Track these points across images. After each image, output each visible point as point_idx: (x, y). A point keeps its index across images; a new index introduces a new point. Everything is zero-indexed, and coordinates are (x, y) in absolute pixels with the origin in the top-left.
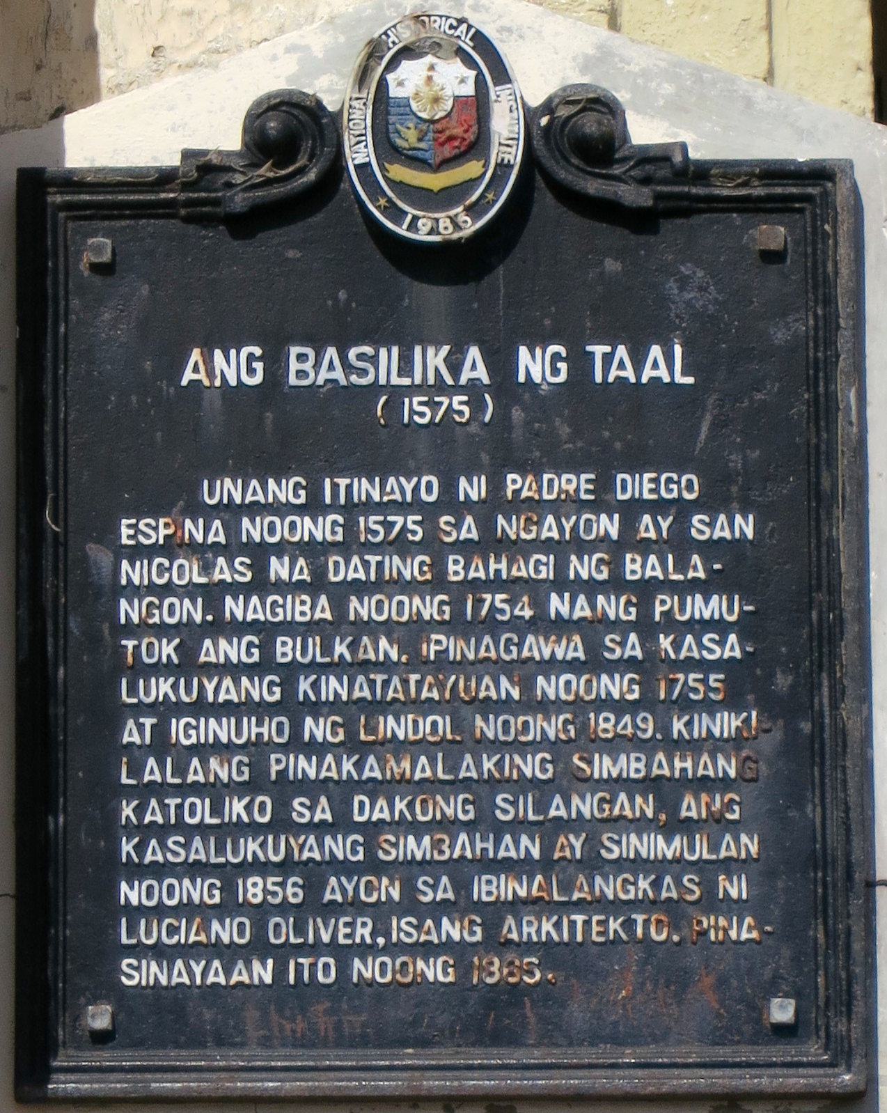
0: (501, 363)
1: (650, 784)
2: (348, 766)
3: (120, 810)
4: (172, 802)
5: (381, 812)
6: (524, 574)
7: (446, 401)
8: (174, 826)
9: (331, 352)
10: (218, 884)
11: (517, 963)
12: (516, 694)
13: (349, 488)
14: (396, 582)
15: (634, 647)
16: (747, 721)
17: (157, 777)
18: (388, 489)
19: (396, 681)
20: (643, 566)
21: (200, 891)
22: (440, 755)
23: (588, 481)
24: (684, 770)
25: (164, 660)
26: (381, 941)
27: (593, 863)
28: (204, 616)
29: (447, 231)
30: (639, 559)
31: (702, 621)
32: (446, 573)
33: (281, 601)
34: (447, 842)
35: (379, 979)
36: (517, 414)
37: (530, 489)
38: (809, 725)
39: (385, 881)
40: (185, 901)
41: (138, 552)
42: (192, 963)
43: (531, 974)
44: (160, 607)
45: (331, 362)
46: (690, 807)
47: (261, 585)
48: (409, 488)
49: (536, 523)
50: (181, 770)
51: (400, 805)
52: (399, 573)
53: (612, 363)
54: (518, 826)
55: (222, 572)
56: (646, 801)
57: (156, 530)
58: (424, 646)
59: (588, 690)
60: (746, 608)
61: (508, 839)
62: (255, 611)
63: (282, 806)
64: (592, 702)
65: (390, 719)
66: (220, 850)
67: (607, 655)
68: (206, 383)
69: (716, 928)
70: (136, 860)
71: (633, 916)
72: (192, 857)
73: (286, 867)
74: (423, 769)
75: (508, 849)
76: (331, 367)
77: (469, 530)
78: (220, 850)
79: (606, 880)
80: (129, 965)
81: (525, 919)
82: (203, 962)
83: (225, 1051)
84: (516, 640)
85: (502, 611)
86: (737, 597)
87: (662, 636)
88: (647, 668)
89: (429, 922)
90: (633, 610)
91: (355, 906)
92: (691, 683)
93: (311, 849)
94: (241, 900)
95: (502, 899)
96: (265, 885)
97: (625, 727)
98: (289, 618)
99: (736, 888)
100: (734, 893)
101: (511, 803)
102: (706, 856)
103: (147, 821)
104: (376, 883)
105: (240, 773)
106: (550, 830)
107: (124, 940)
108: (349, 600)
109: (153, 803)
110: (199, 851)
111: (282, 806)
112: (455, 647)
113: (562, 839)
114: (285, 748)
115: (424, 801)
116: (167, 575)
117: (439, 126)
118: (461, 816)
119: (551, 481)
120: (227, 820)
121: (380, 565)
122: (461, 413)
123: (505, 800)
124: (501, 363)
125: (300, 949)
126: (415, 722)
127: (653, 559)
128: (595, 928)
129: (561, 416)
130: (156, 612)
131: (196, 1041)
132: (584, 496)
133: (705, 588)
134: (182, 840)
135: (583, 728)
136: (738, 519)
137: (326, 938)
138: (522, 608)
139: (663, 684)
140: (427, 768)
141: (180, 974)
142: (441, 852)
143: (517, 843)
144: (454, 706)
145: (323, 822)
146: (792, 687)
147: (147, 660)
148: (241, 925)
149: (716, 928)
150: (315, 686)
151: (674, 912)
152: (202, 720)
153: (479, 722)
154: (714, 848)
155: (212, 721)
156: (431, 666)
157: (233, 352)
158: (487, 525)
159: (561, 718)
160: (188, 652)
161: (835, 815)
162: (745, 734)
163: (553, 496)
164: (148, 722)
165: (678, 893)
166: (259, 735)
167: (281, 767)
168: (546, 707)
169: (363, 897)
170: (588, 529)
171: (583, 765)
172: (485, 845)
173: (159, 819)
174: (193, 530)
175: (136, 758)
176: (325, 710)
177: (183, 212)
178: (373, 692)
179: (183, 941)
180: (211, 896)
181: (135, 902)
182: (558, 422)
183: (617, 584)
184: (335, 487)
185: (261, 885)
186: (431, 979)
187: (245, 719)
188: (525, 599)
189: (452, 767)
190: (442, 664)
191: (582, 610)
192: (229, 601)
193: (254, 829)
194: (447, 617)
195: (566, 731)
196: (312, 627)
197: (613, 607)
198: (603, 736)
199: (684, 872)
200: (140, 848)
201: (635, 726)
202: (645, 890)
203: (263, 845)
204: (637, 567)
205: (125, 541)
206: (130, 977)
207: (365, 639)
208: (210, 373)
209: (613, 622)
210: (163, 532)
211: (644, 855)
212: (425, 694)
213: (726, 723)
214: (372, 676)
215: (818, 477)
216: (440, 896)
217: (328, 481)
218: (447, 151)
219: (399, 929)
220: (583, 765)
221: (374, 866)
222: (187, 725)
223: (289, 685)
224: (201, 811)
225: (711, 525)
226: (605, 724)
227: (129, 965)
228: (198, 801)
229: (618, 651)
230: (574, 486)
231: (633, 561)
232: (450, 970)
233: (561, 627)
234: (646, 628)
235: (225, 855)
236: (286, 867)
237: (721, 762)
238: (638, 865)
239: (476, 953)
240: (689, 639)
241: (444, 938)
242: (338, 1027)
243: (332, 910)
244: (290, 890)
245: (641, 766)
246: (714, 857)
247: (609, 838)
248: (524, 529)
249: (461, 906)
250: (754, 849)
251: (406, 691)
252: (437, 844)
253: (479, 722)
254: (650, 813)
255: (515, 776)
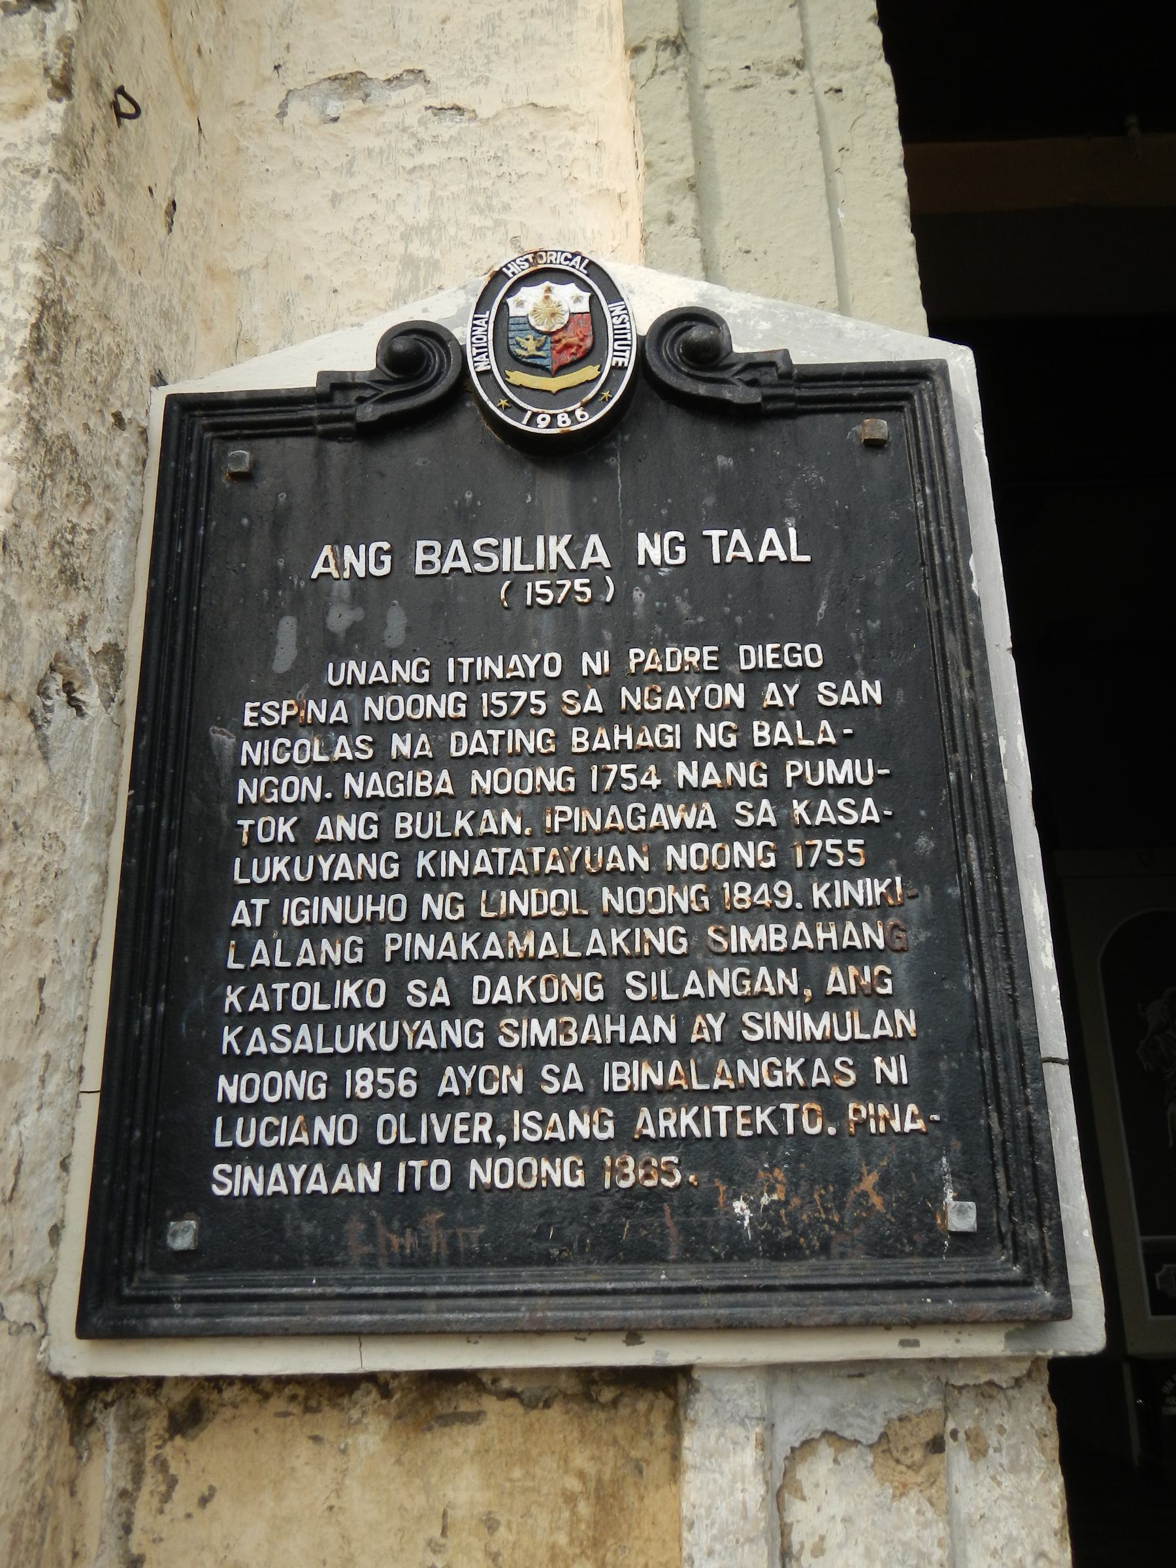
0: (622, 550)
1: (790, 957)
2: (467, 944)
3: (224, 996)
4: (280, 987)
5: (502, 992)
6: (650, 743)
7: (568, 584)
8: (281, 1012)
9: (457, 544)
10: (325, 1076)
11: (654, 1163)
12: (645, 865)
13: (472, 666)
14: (519, 755)
15: (766, 813)
16: (892, 886)
17: (266, 961)
18: (511, 666)
19: (519, 853)
20: (772, 733)
21: (300, 1085)
22: (566, 931)
23: (710, 653)
24: (827, 941)
25: (280, 839)
26: (501, 1139)
27: (734, 1046)
28: (323, 793)
29: (564, 423)
30: (767, 726)
31: (836, 785)
32: (571, 745)
33: (401, 777)
34: (575, 1025)
35: (498, 1184)
36: (638, 596)
37: (653, 662)
38: (958, 891)
39: (507, 1070)
40: (288, 1096)
41: (261, 733)
42: (292, 1168)
43: (670, 1175)
44: (279, 786)
45: (456, 552)
46: (837, 981)
47: (382, 761)
48: (531, 665)
49: (660, 694)
50: (290, 952)
51: (523, 986)
52: (523, 746)
53: (729, 544)
54: (651, 1006)
55: (343, 749)
56: (789, 974)
57: (279, 712)
58: (548, 818)
59: (721, 859)
60: (880, 772)
61: (640, 1020)
62: (375, 788)
63: (397, 991)
64: (725, 870)
65: (513, 895)
66: (328, 1040)
67: (738, 822)
68: (336, 575)
69: (877, 1118)
70: (238, 1051)
71: (782, 1106)
72: (298, 1047)
73: (399, 1056)
74: (548, 946)
75: (641, 1032)
76: (456, 557)
77: (593, 702)
78: (328, 1040)
79: (750, 1065)
80: (222, 1172)
81: (661, 1112)
82: (304, 1167)
83: (323, 1273)
84: (643, 810)
85: (629, 781)
86: (870, 761)
87: (795, 802)
88: (778, 834)
89: (555, 1117)
90: (764, 776)
91: (473, 1100)
92: (829, 850)
93: (426, 1036)
94: (348, 1095)
95: (636, 1088)
96: (375, 1077)
97: (762, 897)
98: (409, 794)
99: (894, 1070)
100: (893, 1077)
101: (643, 981)
102: (859, 1036)
103: (251, 1008)
104: (496, 1072)
105: (353, 954)
106: (687, 1010)
107: (219, 1143)
108: (471, 774)
109: (260, 988)
110: (305, 1040)
111: (397, 991)
112: (581, 818)
113: (699, 1019)
114: (401, 927)
115: (548, 981)
116: (288, 755)
117: (557, 337)
118: (589, 997)
119: (673, 654)
120: (337, 1005)
121: (502, 738)
122: (583, 594)
123: (636, 978)
124: (622, 550)
125: (414, 1151)
126: (539, 896)
127: (781, 725)
128: (741, 1121)
129: (682, 595)
130: (275, 791)
131: (290, 1263)
132: (707, 667)
133: (836, 752)
134: (288, 1028)
135: (717, 898)
136: (865, 684)
137: (440, 1137)
138: (649, 778)
139: (799, 850)
140: (552, 944)
141: (277, 1182)
142: (568, 1037)
143: (650, 1025)
144: (585, 880)
145: (440, 1005)
146: (934, 851)
147: (262, 839)
148: (347, 1123)
149: (877, 1118)
150: (435, 861)
151: (830, 1100)
152: (316, 899)
153: (606, 894)
154: (867, 1026)
155: (326, 901)
156: (557, 838)
157: (362, 548)
158: (610, 696)
159: (694, 888)
160: (306, 828)
161: (999, 986)
162: (891, 901)
163: (678, 668)
164: (259, 903)
165: (831, 1078)
166: (375, 914)
167: (397, 947)
168: (676, 877)
169: (482, 1089)
170: (713, 699)
171: (719, 938)
172: (615, 1028)
173: (265, 1006)
174: (317, 710)
175: (243, 938)
176: (445, 886)
177: (320, 428)
178: (495, 867)
179: (282, 1143)
180: (316, 1090)
181: (233, 1099)
182: (678, 600)
183: (745, 751)
184: (459, 665)
185: (371, 1078)
186: (558, 1183)
187: (361, 898)
188: (652, 768)
189: (579, 942)
190: (567, 835)
191: (711, 777)
192: (349, 778)
193: (365, 1014)
194: (572, 788)
195: (699, 902)
196: (434, 801)
197: (741, 774)
198: (738, 906)
199: (836, 1055)
200: (243, 1039)
201: (773, 896)
202: (793, 1076)
203: (375, 1033)
204: (765, 733)
205: (247, 723)
206: (222, 1185)
207: (487, 813)
208: (340, 567)
209: (743, 789)
210: (285, 713)
211: (791, 1036)
212: (549, 867)
213: (869, 890)
214: (494, 850)
215: (942, 640)
216: (567, 1086)
217: (451, 661)
218: (566, 358)
219: (522, 1125)
220: (719, 938)
221: (494, 1053)
222: (300, 904)
223: (407, 861)
224: (311, 997)
225: (838, 691)
226: (741, 894)
227: (222, 1172)
228: (307, 986)
229: (751, 818)
230: (697, 657)
231: (761, 728)
232: (579, 1172)
233: (691, 794)
234: (778, 794)
235: (333, 1044)
236: (399, 1056)
237: (867, 929)
238: (783, 1046)
239: (607, 1152)
240: (824, 803)
241: (571, 1136)
242: (452, 1240)
243: (448, 1104)
244: (402, 1083)
245: (782, 937)
246: (867, 1037)
247: (751, 1018)
248: (649, 700)
249: (590, 1097)
250: (911, 1027)
251: (530, 865)
252: (563, 1028)
253: (606, 894)
254: (794, 989)
255: (647, 953)
